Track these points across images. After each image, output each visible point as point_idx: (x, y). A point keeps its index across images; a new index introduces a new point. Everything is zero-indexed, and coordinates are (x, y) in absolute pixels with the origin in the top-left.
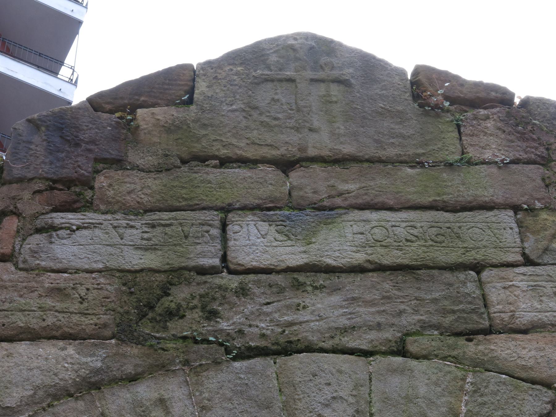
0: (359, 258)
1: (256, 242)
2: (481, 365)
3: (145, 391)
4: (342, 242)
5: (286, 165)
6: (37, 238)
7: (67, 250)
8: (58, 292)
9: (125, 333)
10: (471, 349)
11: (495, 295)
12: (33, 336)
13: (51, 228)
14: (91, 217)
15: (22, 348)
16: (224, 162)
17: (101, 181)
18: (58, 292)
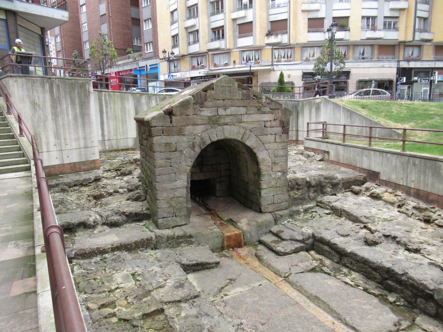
0: (230, 114)
1: (222, 112)
2: (240, 127)
3: (211, 130)
4: (229, 112)
5: (223, 100)
6: (199, 112)
7: (202, 113)
8: (202, 119)
9: (208, 123)
10: (240, 124)
11: (243, 118)
12: (200, 125)
13: (200, 110)
14: (204, 109)
15: (200, 126)
16: (217, 100)
17: (205, 103)
18: (202, 119)
